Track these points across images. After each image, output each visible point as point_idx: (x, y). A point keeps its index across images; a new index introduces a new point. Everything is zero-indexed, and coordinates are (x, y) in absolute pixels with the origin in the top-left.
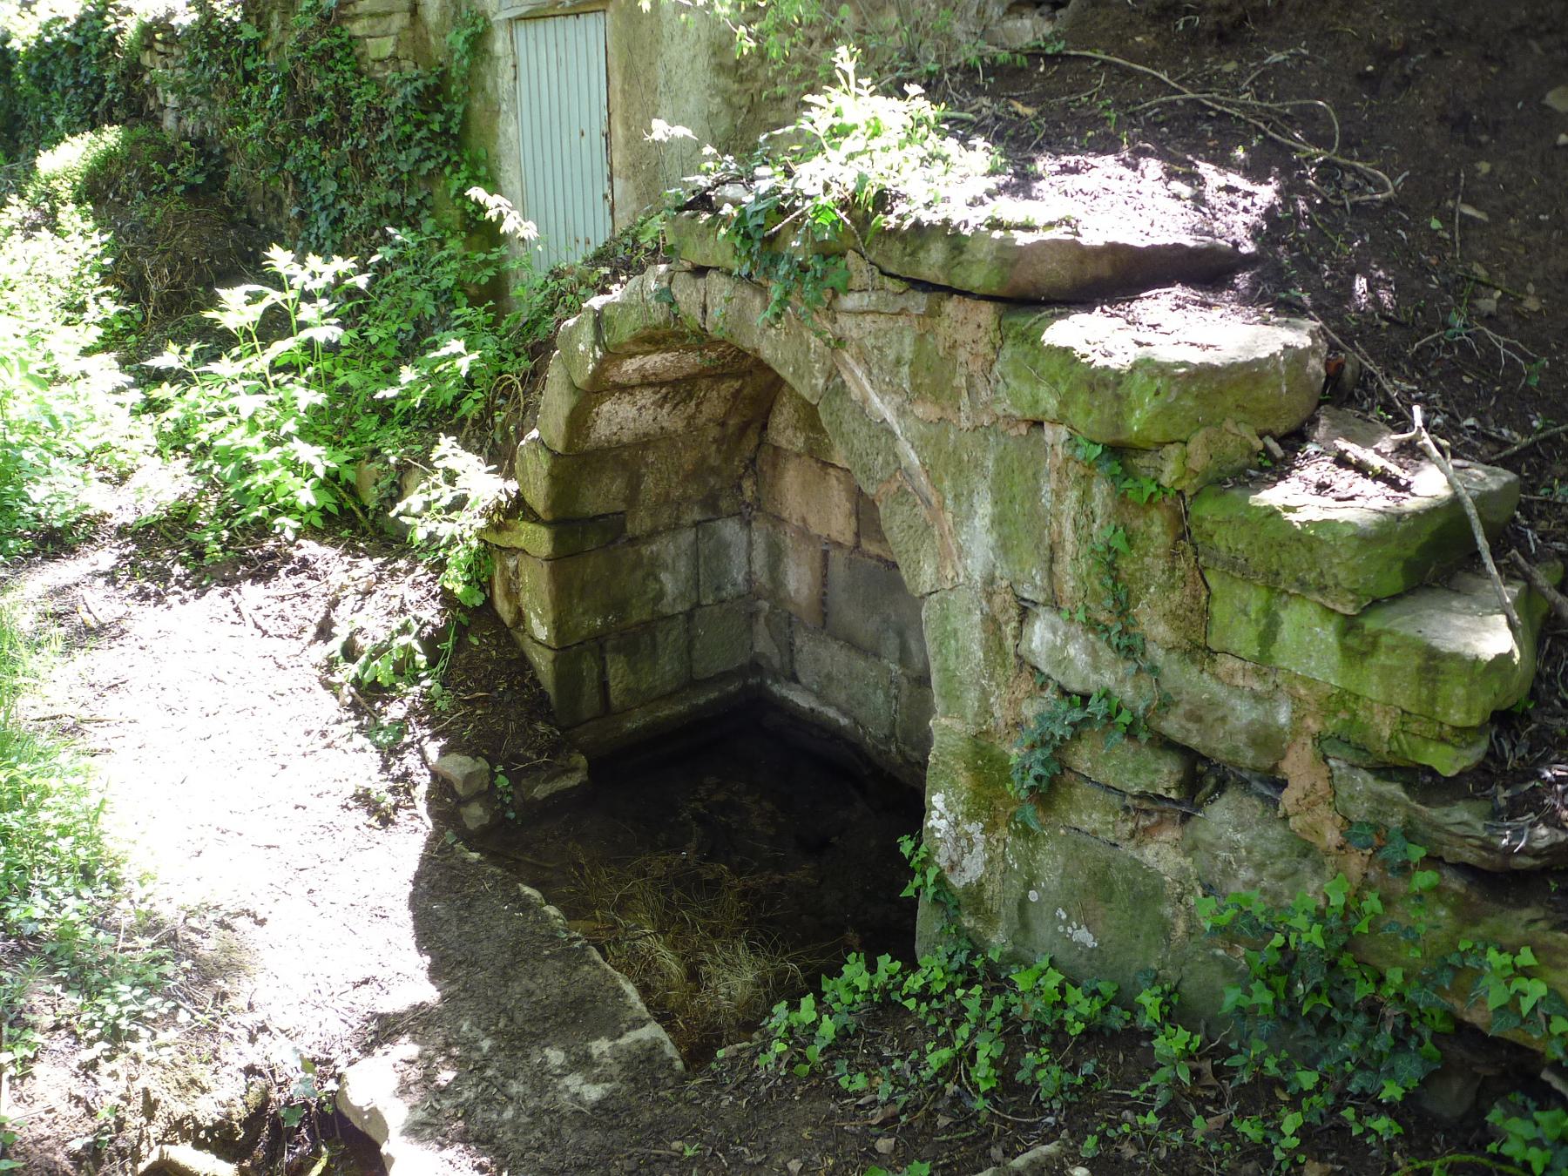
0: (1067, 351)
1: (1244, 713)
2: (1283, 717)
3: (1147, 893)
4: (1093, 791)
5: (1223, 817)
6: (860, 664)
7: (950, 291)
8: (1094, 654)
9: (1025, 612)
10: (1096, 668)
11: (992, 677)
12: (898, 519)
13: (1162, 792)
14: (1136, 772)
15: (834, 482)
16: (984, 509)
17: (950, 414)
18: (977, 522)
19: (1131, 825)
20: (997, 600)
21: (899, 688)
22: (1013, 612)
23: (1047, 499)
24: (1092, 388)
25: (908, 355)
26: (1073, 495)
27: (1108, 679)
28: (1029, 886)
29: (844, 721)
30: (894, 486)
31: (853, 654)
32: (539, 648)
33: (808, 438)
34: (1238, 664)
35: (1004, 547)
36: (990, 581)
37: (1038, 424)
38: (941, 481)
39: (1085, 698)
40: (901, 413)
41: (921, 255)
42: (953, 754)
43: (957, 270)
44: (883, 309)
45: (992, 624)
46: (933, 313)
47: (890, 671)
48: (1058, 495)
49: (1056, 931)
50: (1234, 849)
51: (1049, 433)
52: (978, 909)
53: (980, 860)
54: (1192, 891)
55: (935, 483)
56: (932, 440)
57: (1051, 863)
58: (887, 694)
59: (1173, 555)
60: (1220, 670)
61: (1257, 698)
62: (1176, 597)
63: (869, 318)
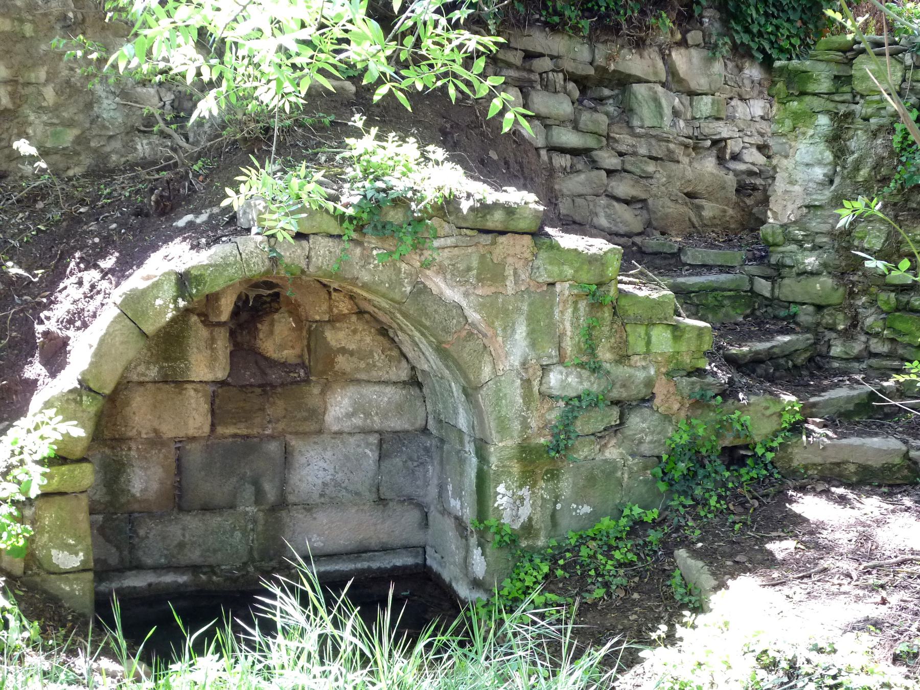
0: (576, 250)
1: (641, 375)
2: (652, 372)
3: (610, 469)
4: (583, 438)
5: (637, 422)
6: (215, 521)
7: (502, 233)
8: (580, 376)
9: (545, 369)
10: (581, 383)
11: (528, 409)
12: (467, 350)
13: (613, 423)
14: (602, 420)
15: (192, 393)
16: (521, 331)
17: (501, 289)
18: (517, 337)
19: (598, 447)
20: (531, 370)
21: (255, 522)
22: (540, 373)
23: (557, 316)
24: (590, 262)
25: (475, 264)
26: (570, 310)
27: (586, 385)
28: (555, 503)
29: (182, 579)
30: (464, 333)
31: (208, 516)
32: (71, 576)
33: (162, 368)
34: (638, 357)
35: (533, 344)
36: (524, 364)
37: (552, 284)
38: (493, 323)
39: (579, 397)
40: (466, 295)
41: (488, 217)
42: (509, 459)
43: (512, 222)
44: (460, 244)
45: (527, 383)
46: (494, 243)
47: (247, 513)
48: (562, 312)
49: (572, 516)
50: (643, 431)
51: (558, 287)
52: (530, 533)
53: (529, 506)
54: (627, 460)
55: (491, 325)
57: (566, 485)
58: (244, 532)
59: (612, 323)
60: (632, 362)
61: (644, 368)
62: (613, 340)
63: (446, 250)
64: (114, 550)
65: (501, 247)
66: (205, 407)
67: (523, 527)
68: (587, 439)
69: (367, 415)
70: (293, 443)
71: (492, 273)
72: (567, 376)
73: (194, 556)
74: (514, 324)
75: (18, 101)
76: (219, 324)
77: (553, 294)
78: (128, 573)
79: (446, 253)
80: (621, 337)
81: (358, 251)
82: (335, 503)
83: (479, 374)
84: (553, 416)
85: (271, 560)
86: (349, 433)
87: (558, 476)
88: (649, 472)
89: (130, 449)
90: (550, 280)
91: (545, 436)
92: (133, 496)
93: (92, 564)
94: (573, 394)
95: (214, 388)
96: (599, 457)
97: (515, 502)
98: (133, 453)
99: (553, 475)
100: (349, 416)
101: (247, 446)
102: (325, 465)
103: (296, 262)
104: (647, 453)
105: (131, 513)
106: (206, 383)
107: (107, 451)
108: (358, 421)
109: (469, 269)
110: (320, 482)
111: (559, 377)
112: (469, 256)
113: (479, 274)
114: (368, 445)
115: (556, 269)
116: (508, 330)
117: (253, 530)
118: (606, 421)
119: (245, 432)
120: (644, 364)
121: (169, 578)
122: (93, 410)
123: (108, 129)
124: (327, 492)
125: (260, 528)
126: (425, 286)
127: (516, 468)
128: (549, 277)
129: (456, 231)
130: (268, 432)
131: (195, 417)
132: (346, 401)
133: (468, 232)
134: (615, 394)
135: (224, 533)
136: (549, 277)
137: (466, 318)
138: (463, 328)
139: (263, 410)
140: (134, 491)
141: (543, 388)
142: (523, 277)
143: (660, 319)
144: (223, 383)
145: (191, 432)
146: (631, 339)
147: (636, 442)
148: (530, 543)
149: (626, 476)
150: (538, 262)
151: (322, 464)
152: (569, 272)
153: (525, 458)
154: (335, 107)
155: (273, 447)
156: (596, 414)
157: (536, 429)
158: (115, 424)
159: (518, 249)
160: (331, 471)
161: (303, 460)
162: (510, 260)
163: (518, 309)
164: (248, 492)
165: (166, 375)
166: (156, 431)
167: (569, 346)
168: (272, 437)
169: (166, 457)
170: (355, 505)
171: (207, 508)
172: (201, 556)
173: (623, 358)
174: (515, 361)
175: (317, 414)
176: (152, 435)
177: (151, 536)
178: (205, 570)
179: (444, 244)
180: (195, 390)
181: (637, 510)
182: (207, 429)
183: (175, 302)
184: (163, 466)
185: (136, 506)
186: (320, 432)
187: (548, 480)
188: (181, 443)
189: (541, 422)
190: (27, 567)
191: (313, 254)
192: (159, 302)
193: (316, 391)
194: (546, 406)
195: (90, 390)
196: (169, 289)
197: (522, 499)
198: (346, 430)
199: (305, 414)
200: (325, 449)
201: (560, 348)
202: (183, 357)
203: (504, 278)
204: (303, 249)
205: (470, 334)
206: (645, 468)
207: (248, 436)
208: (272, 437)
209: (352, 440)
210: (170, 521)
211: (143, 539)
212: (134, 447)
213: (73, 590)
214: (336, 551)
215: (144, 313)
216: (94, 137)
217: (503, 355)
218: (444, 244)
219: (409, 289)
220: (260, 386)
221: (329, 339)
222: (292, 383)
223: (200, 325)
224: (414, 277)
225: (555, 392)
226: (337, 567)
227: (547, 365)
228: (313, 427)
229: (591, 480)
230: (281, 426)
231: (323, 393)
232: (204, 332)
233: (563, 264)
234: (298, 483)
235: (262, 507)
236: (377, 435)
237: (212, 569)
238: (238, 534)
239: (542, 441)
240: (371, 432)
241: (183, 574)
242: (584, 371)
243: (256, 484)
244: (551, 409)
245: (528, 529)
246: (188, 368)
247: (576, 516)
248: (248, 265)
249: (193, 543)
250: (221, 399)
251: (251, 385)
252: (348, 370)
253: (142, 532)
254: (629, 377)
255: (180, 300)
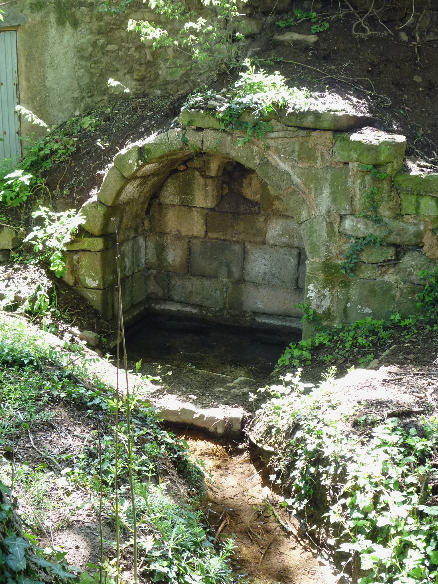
0: (359, 142)
1: (412, 229)
2: (422, 228)
3: (387, 288)
4: (367, 265)
5: (408, 260)
6: (207, 283)
7: (314, 130)
8: (366, 224)
9: (342, 218)
10: (367, 229)
11: (330, 241)
12: (292, 200)
13: (390, 258)
14: (382, 255)
15: (195, 213)
16: (326, 192)
17: (313, 165)
18: (324, 195)
19: (380, 272)
20: (332, 217)
21: (227, 287)
22: (338, 219)
23: (350, 184)
24: (368, 150)
25: (297, 148)
26: (359, 181)
27: (371, 231)
28: (347, 302)
29: (194, 311)
30: (291, 190)
31: (204, 280)
32: (93, 291)
33: (181, 198)
34: (410, 216)
35: (334, 201)
36: (329, 212)
37: (347, 163)
38: (309, 185)
39: (364, 238)
40: (293, 167)
41: (304, 119)
42: (317, 270)
43: (319, 123)
44: (287, 136)
45: (330, 225)
46: (308, 136)
47: (223, 282)
48: (354, 182)
49: (358, 313)
50: (412, 266)
51: (351, 166)
52: (328, 318)
53: (329, 301)
54: (400, 284)
55: (307, 186)
56: (304, 174)
57: (354, 292)
58: (222, 292)
59: (390, 192)
60: (405, 219)
61: (415, 224)
62: (391, 203)
63: (280, 139)
64: (160, 289)
65: (313, 138)
66: (201, 221)
67: (324, 313)
68: (371, 265)
69: (291, 237)
70: (248, 247)
71: (307, 154)
72: (357, 223)
73: (197, 300)
74: (321, 187)
75: (155, 57)
76: (211, 177)
77: (348, 170)
78: (168, 302)
79: (280, 141)
80: (397, 202)
81: (229, 138)
82: (269, 284)
83: (299, 216)
84: (346, 247)
85: (235, 310)
86: (281, 247)
87: (349, 286)
88: (416, 295)
89: (167, 239)
90: (346, 161)
91: (341, 259)
92: (169, 263)
93: (102, 287)
94: (361, 235)
95: (207, 212)
96: (380, 279)
97: (319, 297)
98: (169, 241)
99: (346, 284)
100: (280, 236)
101: (223, 245)
102: (266, 263)
103: (196, 144)
104: (416, 282)
105: (169, 272)
106: (204, 208)
107: (158, 238)
108: (285, 239)
109: (293, 151)
110: (262, 271)
111: (351, 223)
112: (294, 143)
113: (299, 155)
114: (291, 254)
115: (346, 154)
116: (319, 190)
117: (226, 292)
118: (384, 256)
119: (222, 237)
120: (415, 221)
121: (188, 309)
122: (102, 212)
123: (200, 69)
124: (267, 278)
125: (230, 291)
126: (268, 161)
127: (321, 276)
128: (341, 158)
129: (285, 128)
130: (235, 239)
131: (196, 226)
132: (278, 227)
133: (291, 129)
134: (392, 239)
135: (211, 291)
136: (341, 158)
137: (292, 181)
138: (290, 187)
139: (232, 226)
140: (169, 260)
141: (341, 229)
142: (327, 158)
143: (426, 192)
144: (212, 209)
145: (195, 234)
146: (404, 204)
147: (408, 273)
148: (329, 323)
149: (398, 294)
150: (335, 149)
151: (263, 261)
152: (355, 156)
153: (328, 271)
154: (296, 52)
155: (237, 248)
156: (377, 249)
157: (335, 254)
158: (161, 225)
159: (323, 140)
160: (269, 266)
161: (253, 258)
162: (319, 147)
163: (324, 178)
164: (224, 271)
165: (183, 202)
166: (178, 231)
167: (358, 205)
168: (237, 242)
169: (183, 245)
170: (283, 288)
171: (203, 276)
172: (200, 300)
173: (399, 216)
174: (323, 209)
175: (262, 233)
176: (177, 233)
177: (177, 285)
178: (205, 308)
179: (277, 137)
180: (197, 211)
181: (397, 317)
182: (203, 233)
183: (138, 162)
184: (182, 250)
185: (170, 269)
186: (264, 243)
187: (342, 287)
188: (191, 239)
189: (339, 251)
190: (75, 284)
191: (205, 139)
192: (130, 161)
193: (262, 219)
194: (342, 241)
195: (101, 203)
196: (135, 155)
197: (324, 296)
198: (278, 244)
199: (255, 232)
200: (266, 253)
201: (352, 205)
202: (191, 194)
203: (316, 158)
204: (199, 136)
205: (294, 191)
206: (413, 292)
207: (224, 240)
208: (237, 242)
209: (282, 250)
210: (186, 279)
211: (173, 286)
212: (169, 237)
213: (93, 297)
214: (270, 312)
215: (124, 167)
216: (193, 74)
217: (315, 205)
218: (277, 137)
219: (258, 161)
220: (231, 213)
221: (270, 190)
222: (249, 214)
223: (200, 177)
224: (261, 155)
225: (349, 233)
226: (272, 322)
227: (345, 215)
228: (259, 239)
229: (373, 292)
230: (241, 237)
231: (266, 221)
232: (201, 181)
233: (350, 151)
234: (251, 270)
235: (231, 280)
236: (298, 250)
237: (207, 309)
238: (218, 293)
239: (340, 262)
240: (293, 247)
241: (195, 308)
242: (369, 221)
243: (228, 266)
244: (345, 243)
245: (327, 314)
246: (194, 200)
247: (360, 313)
248: (172, 144)
249: (196, 293)
250: (211, 217)
251: (227, 212)
252: (281, 209)
253: (173, 282)
254: (403, 229)
255: (140, 161)
